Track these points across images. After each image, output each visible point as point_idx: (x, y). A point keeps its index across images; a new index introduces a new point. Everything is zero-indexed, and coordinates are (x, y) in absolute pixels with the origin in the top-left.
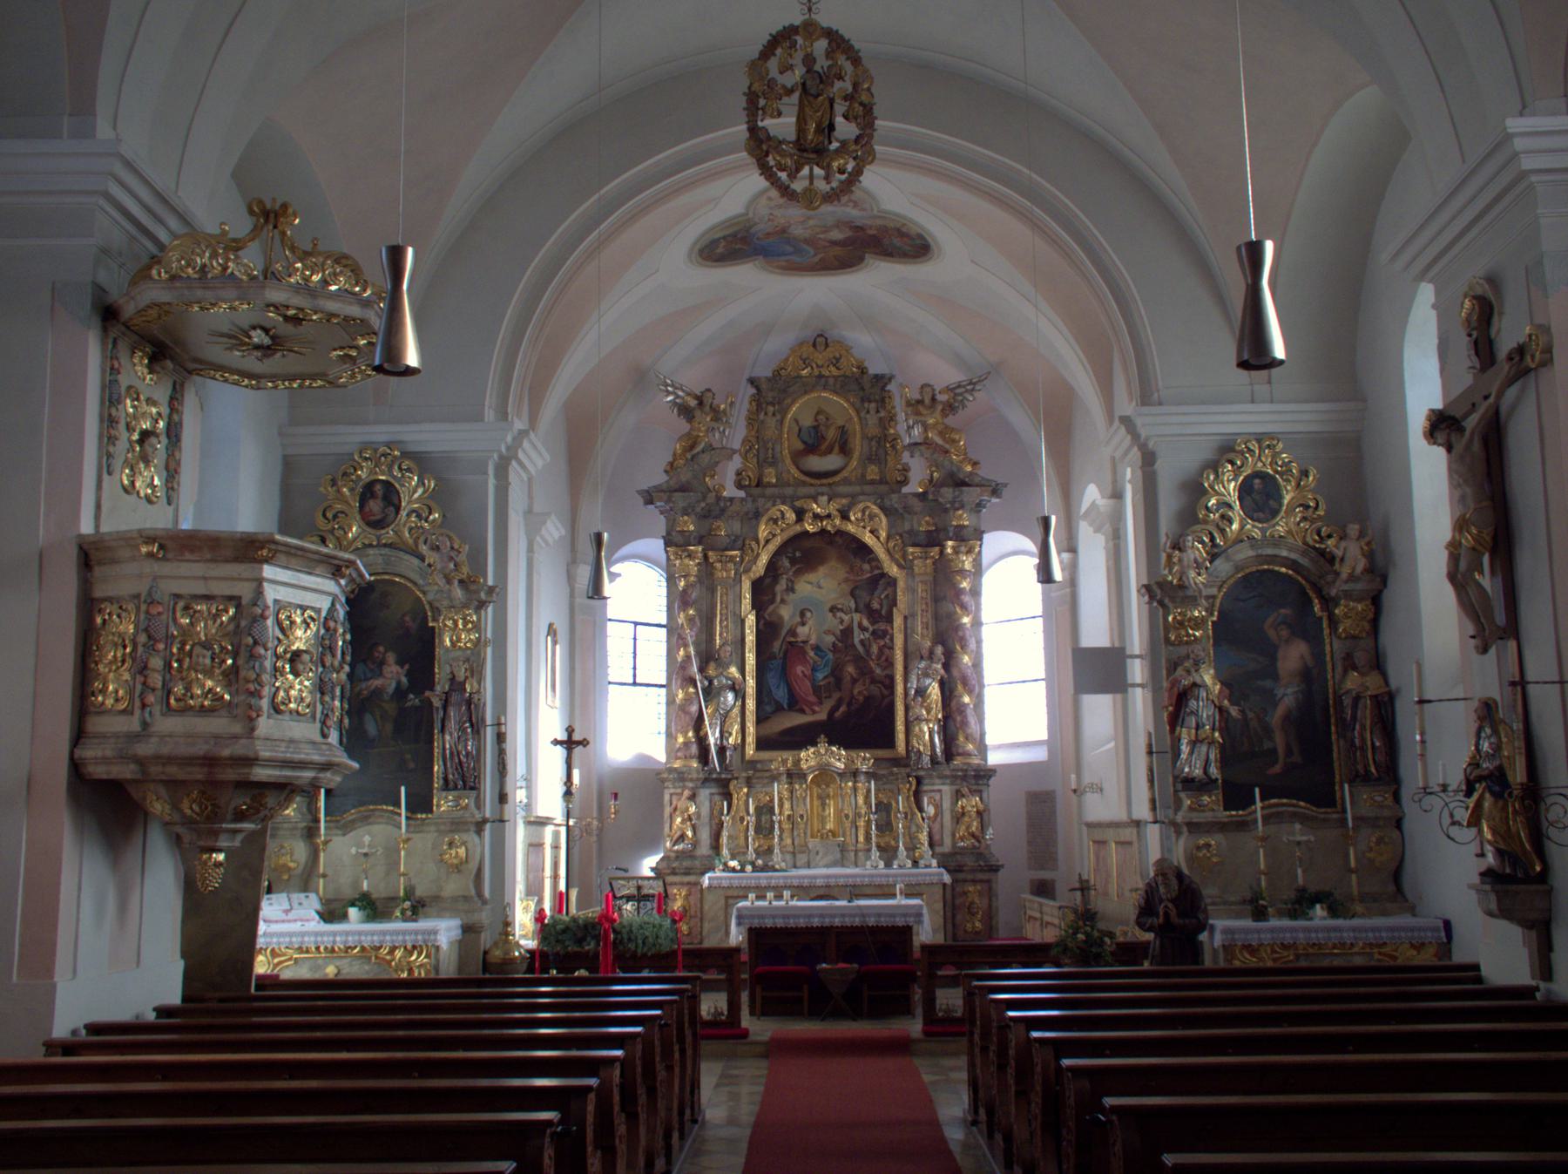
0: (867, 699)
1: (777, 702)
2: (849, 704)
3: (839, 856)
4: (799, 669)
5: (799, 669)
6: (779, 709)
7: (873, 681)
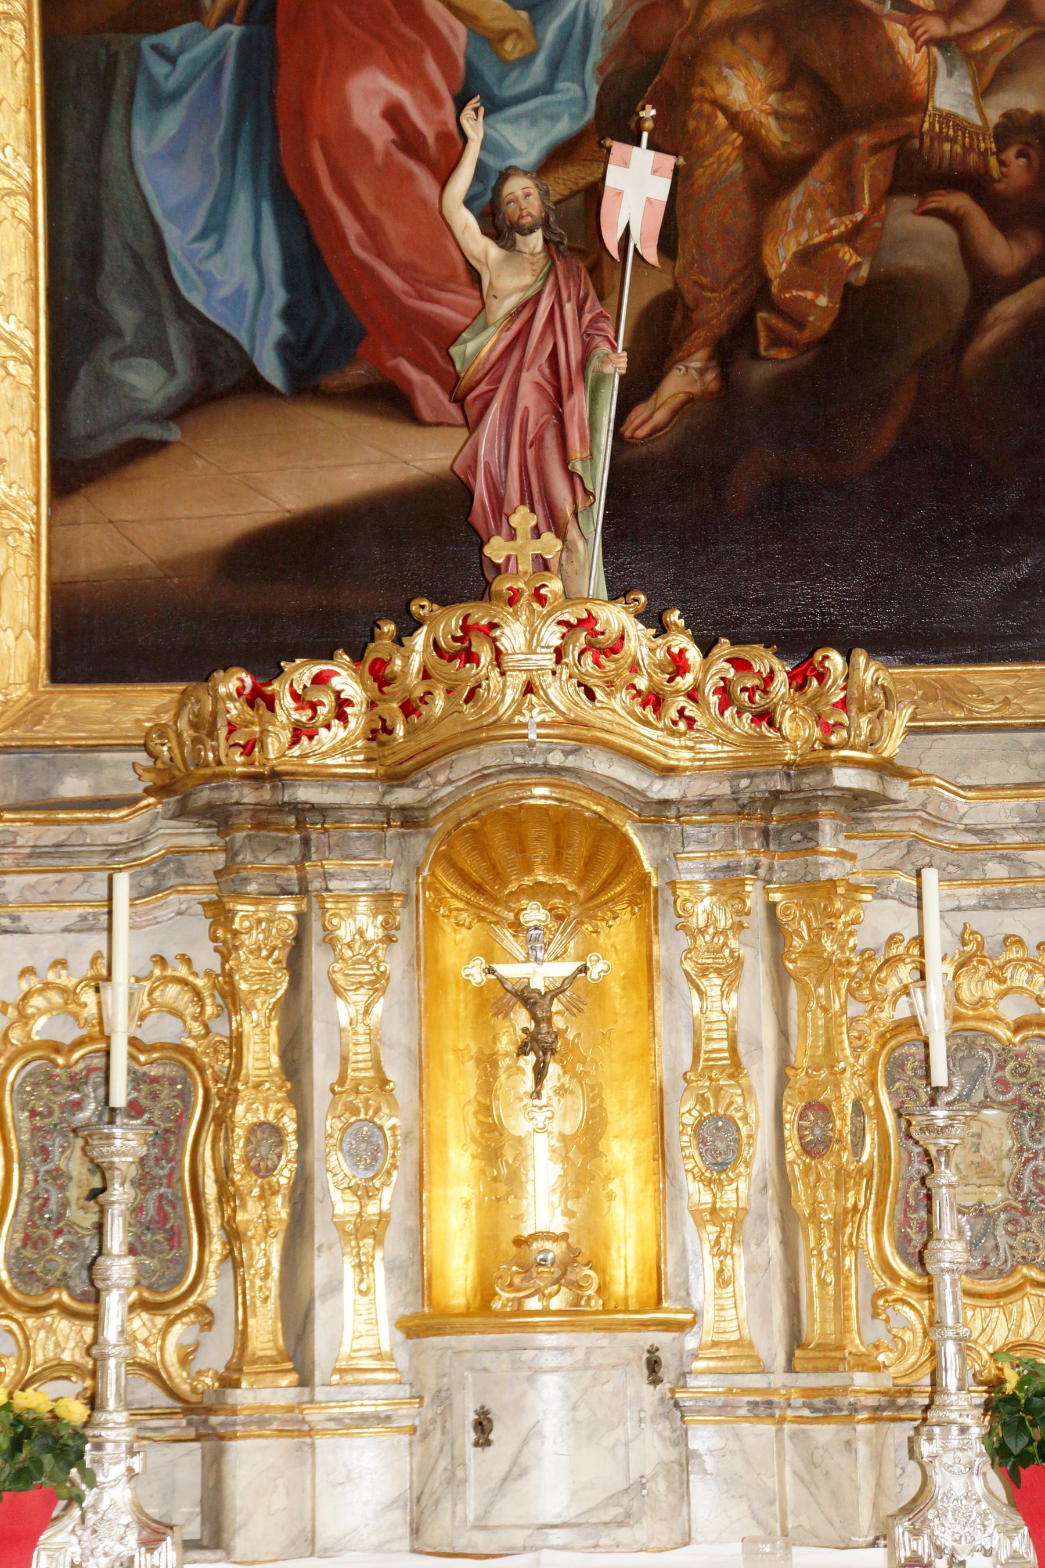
0: (876, 307)
1: (211, 343)
2: (732, 347)
3: (651, 1449)
4: (370, 95)
5: (370, 95)
6: (220, 381)
7: (916, 175)
